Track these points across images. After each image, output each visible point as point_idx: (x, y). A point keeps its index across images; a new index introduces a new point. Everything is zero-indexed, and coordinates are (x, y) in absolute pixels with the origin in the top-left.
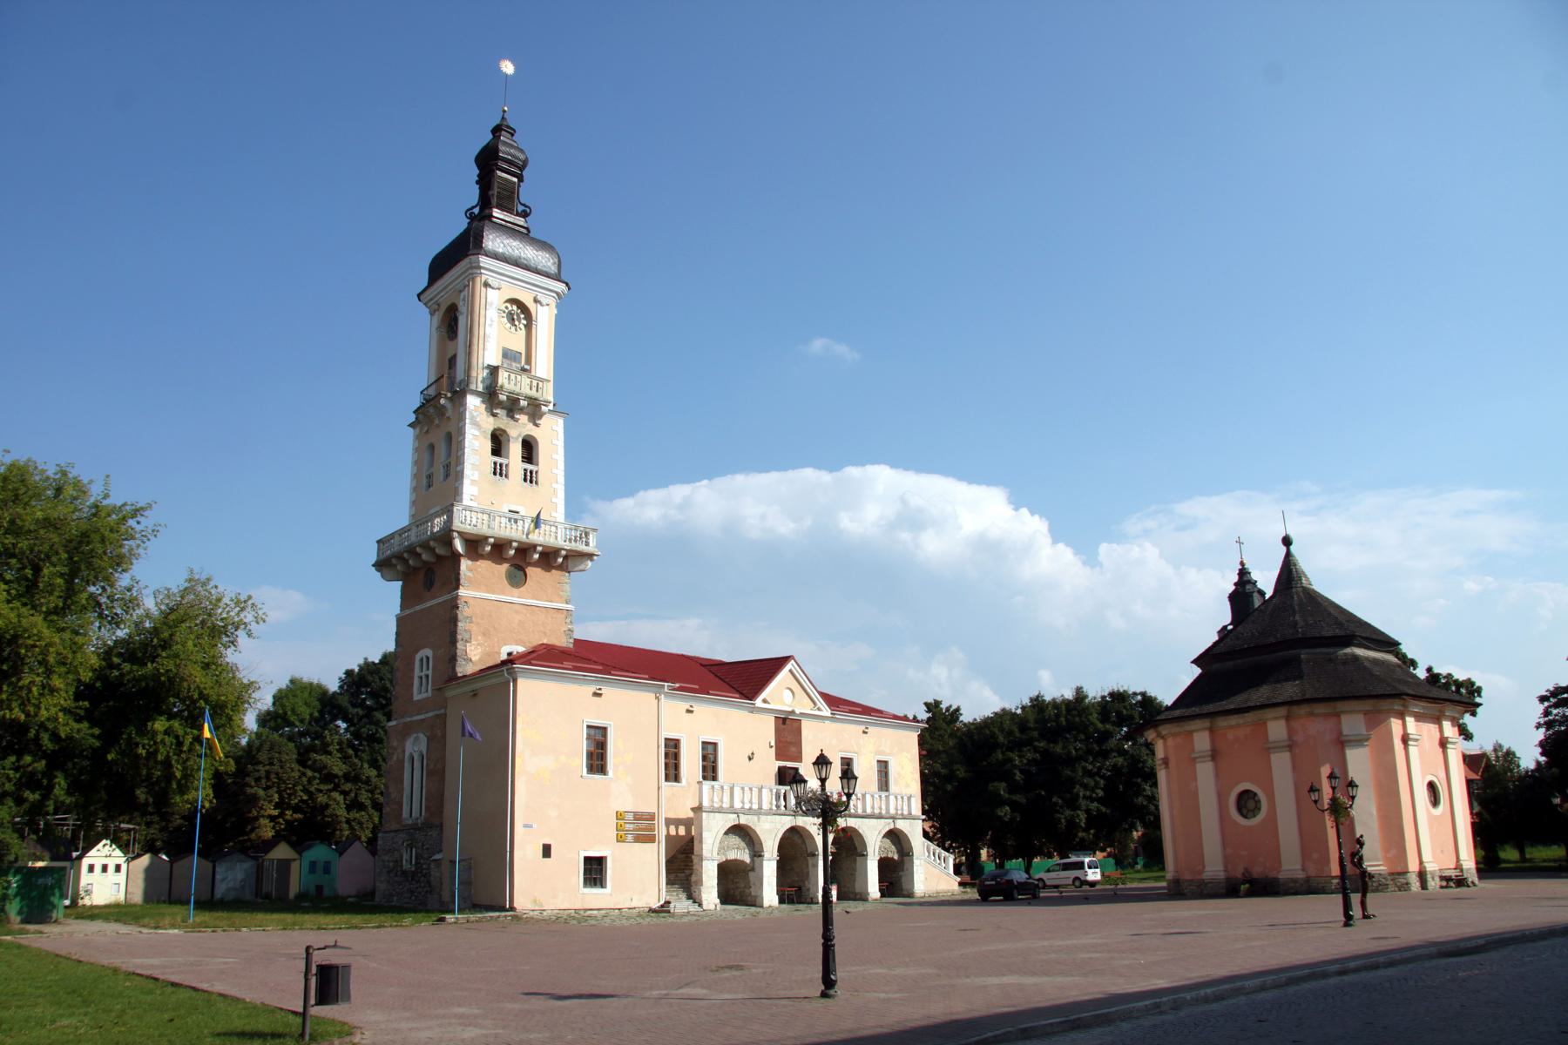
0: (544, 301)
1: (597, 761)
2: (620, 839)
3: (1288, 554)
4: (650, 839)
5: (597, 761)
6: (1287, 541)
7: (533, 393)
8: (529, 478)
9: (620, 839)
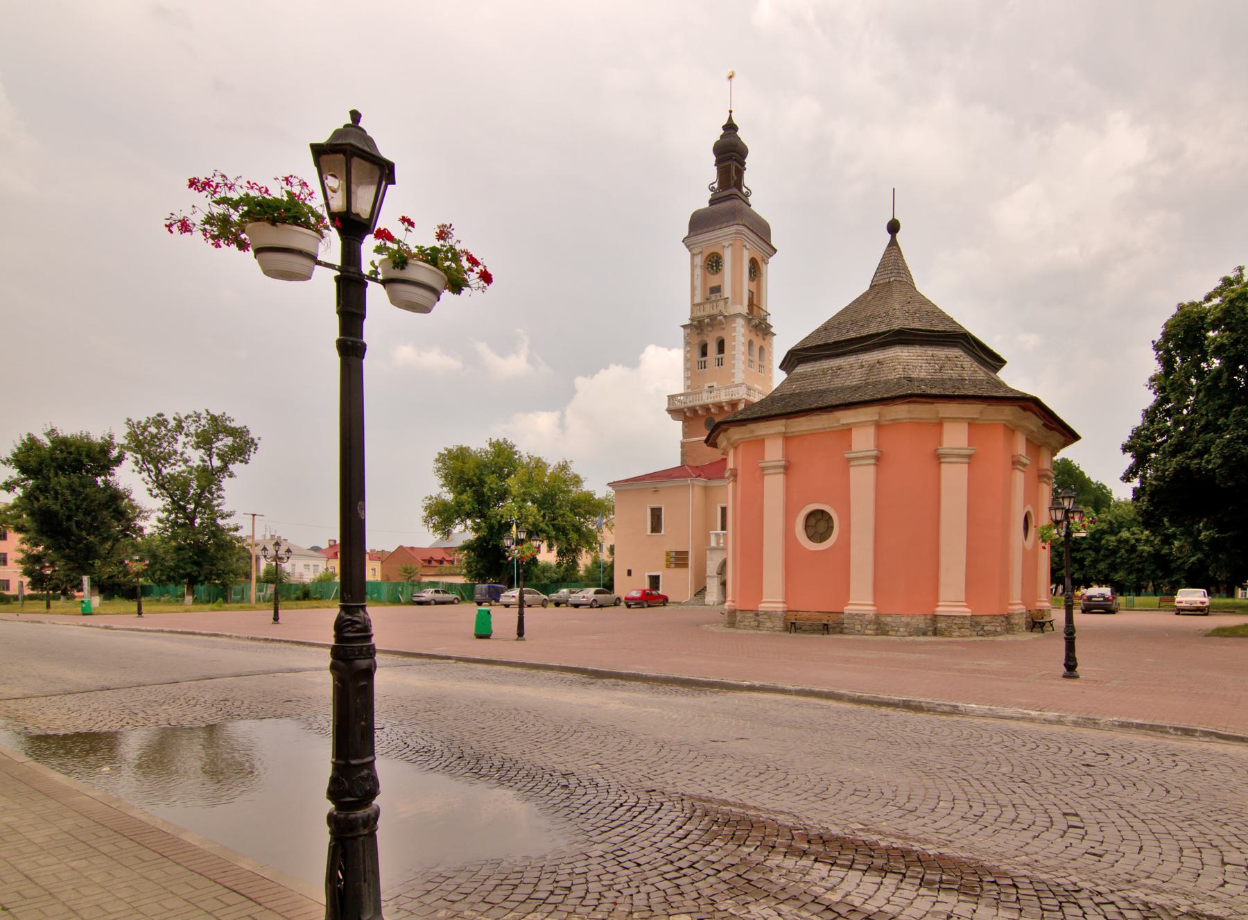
0: (726, 244)
1: (656, 526)
2: (668, 566)
3: (893, 243)
4: (686, 566)
5: (656, 526)
6: (893, 227)
7: (712, 312)
8: (720, 363)
9: (668, 566)
